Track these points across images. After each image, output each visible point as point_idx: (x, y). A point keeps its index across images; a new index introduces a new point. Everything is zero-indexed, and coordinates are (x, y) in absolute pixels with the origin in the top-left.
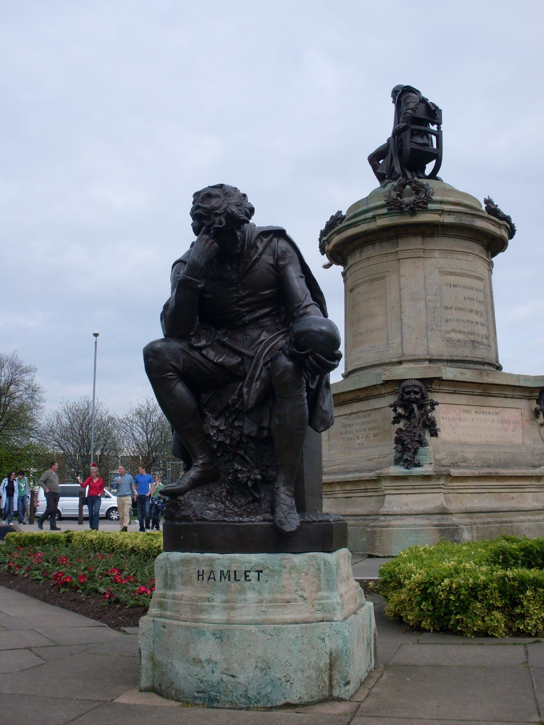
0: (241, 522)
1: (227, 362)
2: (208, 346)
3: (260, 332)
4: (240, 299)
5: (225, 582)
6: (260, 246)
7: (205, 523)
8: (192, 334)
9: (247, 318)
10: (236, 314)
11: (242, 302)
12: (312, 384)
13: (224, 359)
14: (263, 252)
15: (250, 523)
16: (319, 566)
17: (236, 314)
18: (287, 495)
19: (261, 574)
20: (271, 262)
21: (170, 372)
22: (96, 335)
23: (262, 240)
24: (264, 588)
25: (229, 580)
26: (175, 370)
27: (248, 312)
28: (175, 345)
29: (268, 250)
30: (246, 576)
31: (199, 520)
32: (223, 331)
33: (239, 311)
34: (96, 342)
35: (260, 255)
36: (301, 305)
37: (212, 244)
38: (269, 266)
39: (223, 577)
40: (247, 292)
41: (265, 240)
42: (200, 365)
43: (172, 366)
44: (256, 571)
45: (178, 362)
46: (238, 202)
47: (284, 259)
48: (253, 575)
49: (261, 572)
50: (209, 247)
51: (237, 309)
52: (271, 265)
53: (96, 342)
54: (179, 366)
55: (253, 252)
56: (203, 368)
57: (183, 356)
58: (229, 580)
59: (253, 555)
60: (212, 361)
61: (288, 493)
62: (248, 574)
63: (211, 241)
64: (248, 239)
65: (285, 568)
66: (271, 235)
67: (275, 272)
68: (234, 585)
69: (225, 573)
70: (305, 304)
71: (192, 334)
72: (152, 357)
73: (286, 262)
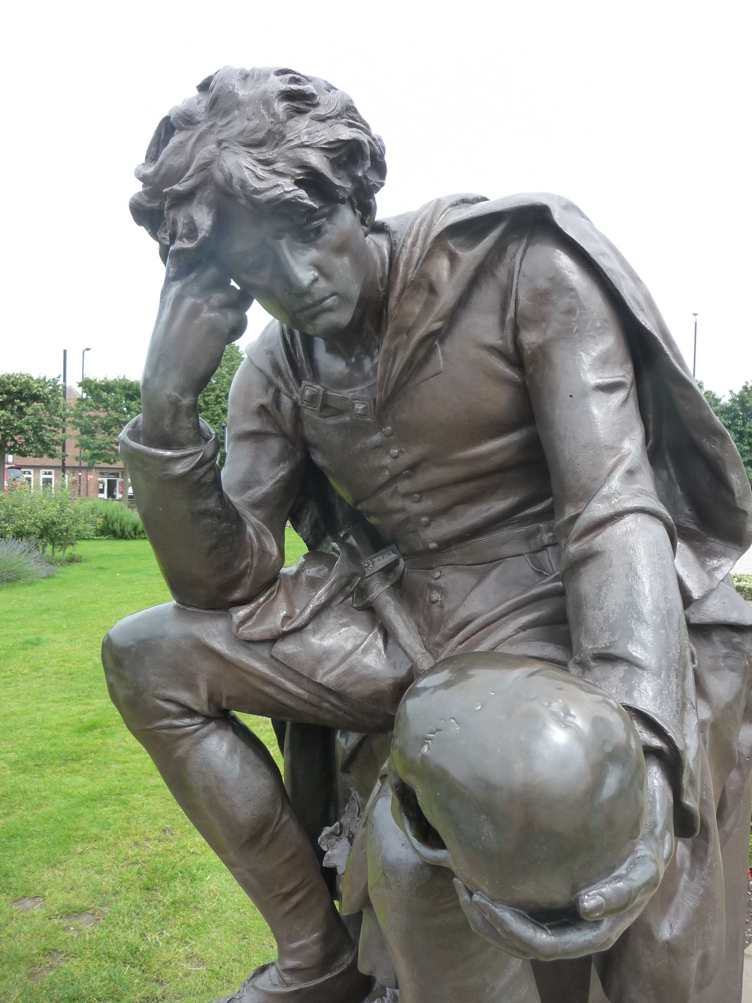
4: (395, 478)
8: (237, 595)
14: (463, 302)
17: (398, 517)
20: (493, 338)
22: (695, 315)
27: (434, 515)
29: (487, 296)
35: (452, 317)
36: (577, 517)
37: (195, 312)
41: (471, 256)
45: (190, 686)
46: (255, 131)
47: (539, 320)
51: (397, 503)
52: (493, 349)
55: (417, 309)
56: (281, 697)
63: (189, 302)
66: (495, 234)
70: (598, 509)
71: (237, 595)
73: (550, 333)
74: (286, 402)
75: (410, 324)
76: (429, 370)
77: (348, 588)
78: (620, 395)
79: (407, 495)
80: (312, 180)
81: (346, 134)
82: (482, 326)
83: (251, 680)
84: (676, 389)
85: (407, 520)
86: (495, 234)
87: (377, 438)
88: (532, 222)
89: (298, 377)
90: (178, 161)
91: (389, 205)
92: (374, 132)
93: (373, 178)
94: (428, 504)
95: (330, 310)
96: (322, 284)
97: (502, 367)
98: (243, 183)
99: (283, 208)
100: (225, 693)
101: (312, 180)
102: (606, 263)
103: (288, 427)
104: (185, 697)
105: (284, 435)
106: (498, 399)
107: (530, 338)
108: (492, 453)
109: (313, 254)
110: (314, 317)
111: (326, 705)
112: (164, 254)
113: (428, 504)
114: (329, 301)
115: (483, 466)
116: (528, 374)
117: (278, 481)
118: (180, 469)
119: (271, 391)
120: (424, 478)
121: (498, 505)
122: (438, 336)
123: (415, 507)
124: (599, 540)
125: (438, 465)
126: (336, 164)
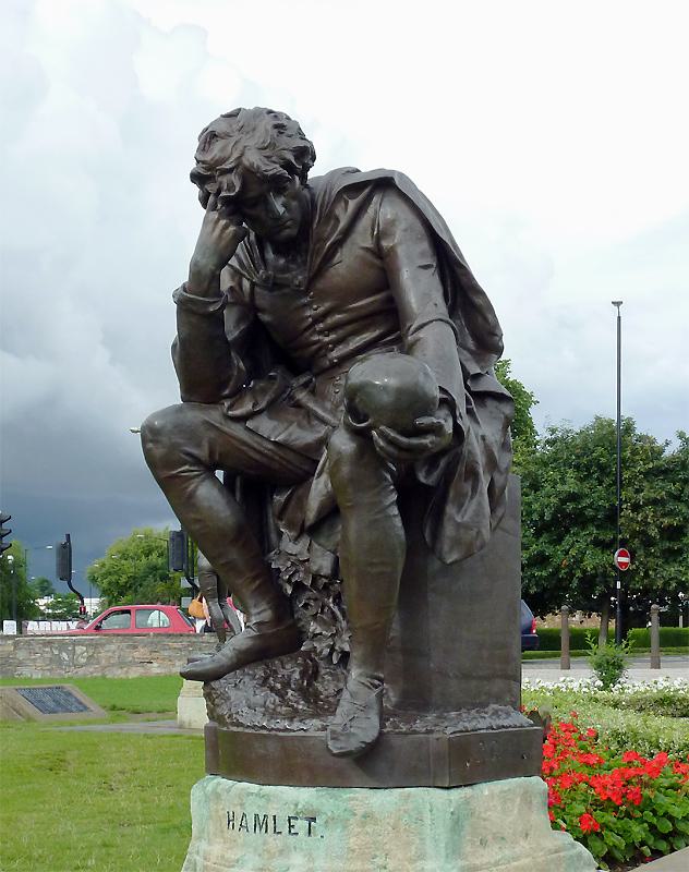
0: (286, 730)
1: (296, 439)
2: (260, 412)
3: (349, 382)
4: (317, 320)
5: (260, 836)
6: (344, 215)
7: (240, 729)
8: (227, 392)
9: (335, 354)
10: (315, 347)
11: (321, 325)
12: (429, 473)
13: (290, 435)
15: (302, 733)
16: (420, 813)
17: (315, 347)
21: (185, 464)
22: (618, 304)
24: (318, 848)
26: (196, 461)
27: (337, 343)
28: (196, 416)
31: (233, 724)
32: (303, 380)
34: (619, 317)
37: (226, 227)
39: (258, 826)
40: (327, 305)
41: (352, 204)
42: (244, 448)
43: (188, 454)
44: (307, 819)
45: (199, 445)
48: (301, 825)
49: (314, 819)
50: (220, 236)
51: (316, 338)
52: (367, 249)
53: (619, 317)
54: (203, 453)
56: (252, 454)
59: (303, 789)
60: (268, 439)
63: (223, 222)
64: (322, 206)
66: (367, 191)
68: (274, 842)
69: (261, 818)
71: (227, 392)
72: (151, 441)
74: (246, 284)
78: (433, 270)
79: (321, 332)
80: (287, 165)
83: (234, 442)
84: (459, 271)
85: (320, 349)
87: (306, 300)
88: (385, 184)
91: (311, 174)
94: (333, 336)
95: (289, 227)
96: (287, 214)
98: (258, 167)
99: (276, 179)
100: (218, 450)
101: (287, 165)
102: (420, 206)
103: (247, 299)
104: (195, 451)
106: (371, 275)
107: (385, 244)
109: (282, 199)
110: (280, 231)
111: (277, 458)
112: (204, 201)
113: (333, 336)
114: (289, 223)
119: (237, 278)
120: (330, 321)
121: (368, 336)
122: (339, 244)
123: (327, 339)
124: (421, 334)
126: (296, 158)
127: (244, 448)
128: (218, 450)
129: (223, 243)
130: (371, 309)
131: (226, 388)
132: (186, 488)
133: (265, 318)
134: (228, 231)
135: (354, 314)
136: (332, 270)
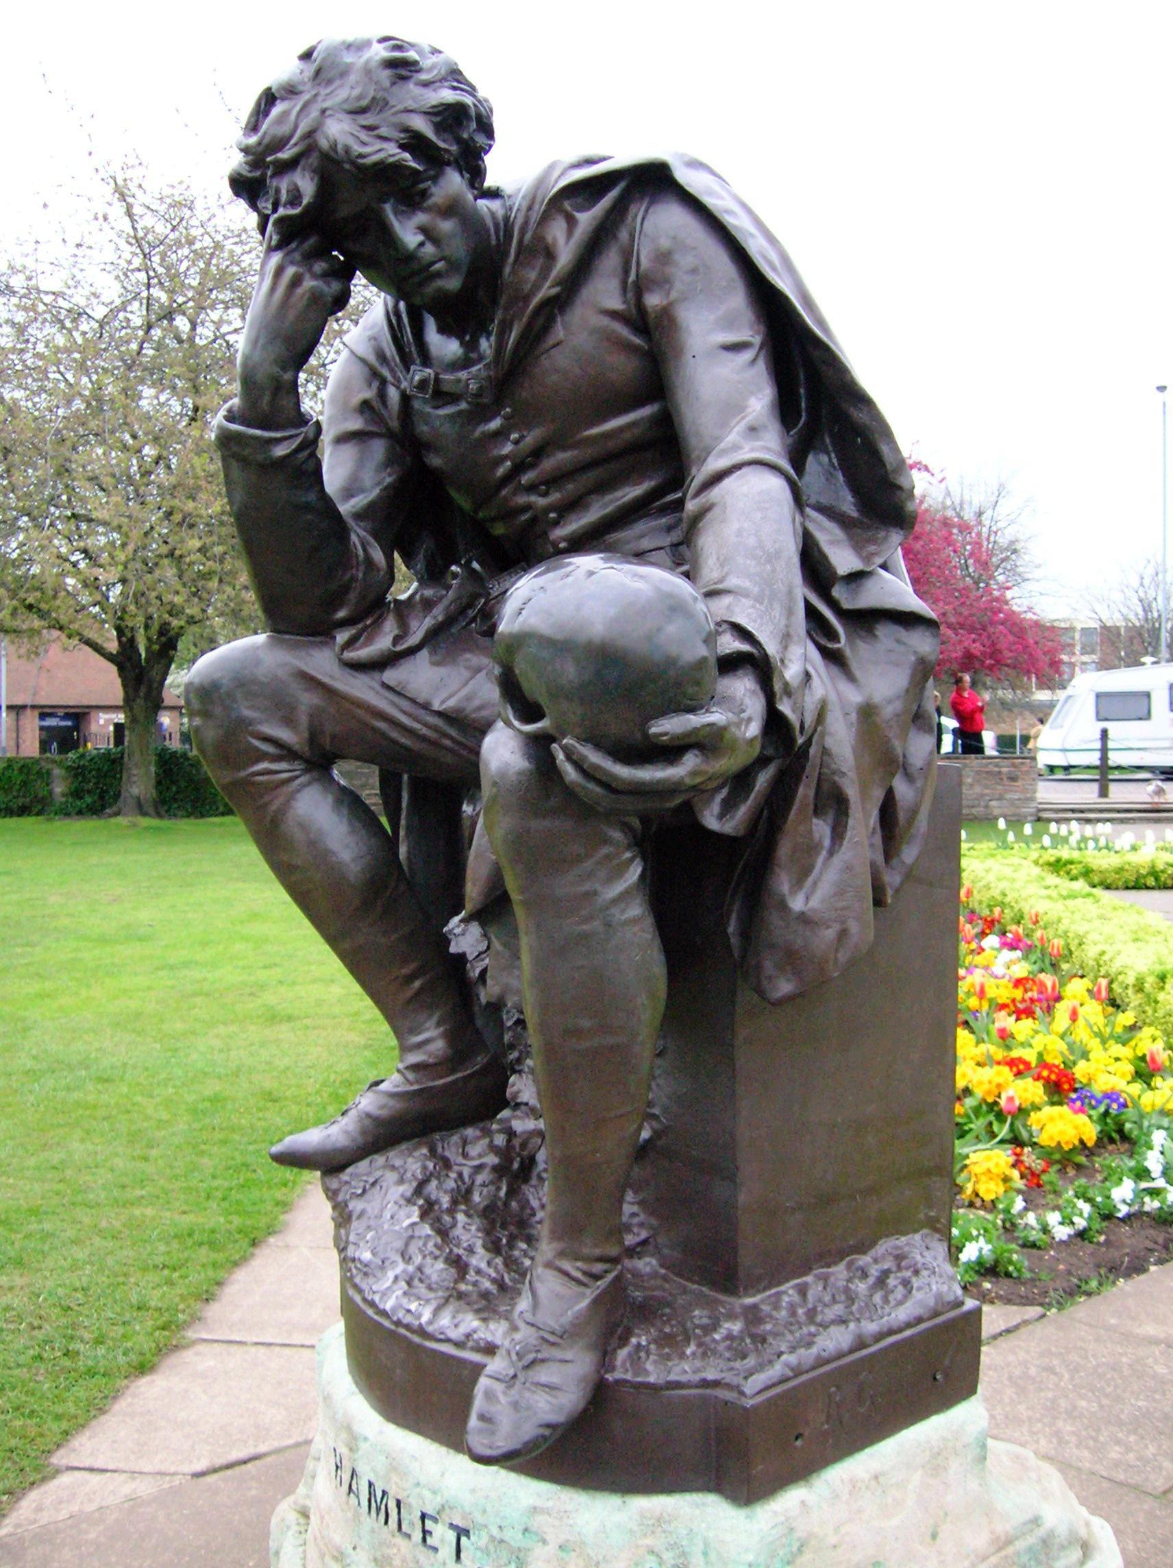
4: (520, 467)
8: (341, 614)
10: (525, 517)
12: (728, 806)
17: (525, 517)
18: (567, 1274)
19: (464, 1539)
20: (616, 304)
22: (1162, 389)
23: (571, 222)
25: (386, 1522)
26: (286, 752)
29: (610, 261)
30: (425, 1533)
33: (528, 507)
37: (296, 282)
38: (606, 321)
41: (587, 219)
42: (382, 725)
44: (452, 1526)
45: (289, 721)
46: (359, 98)
48: (442, 1535)
49: (467, 1533)
51: (522, 500)
52: (614, 314)
56: (394, 734)
57: (307, 700)
58: (386, 1522)
60: (426, 706)
61: (567, 1265)
62: (429, 1524)
63: (291, 271)
65: (544, 1542)
66: (613, 194)
67: (637, 341)
70: (715, 464)
71: (341, 614)
74: (393, 394)
75: (526, 291)
76: (551, 341)
77: (470, 612)
78: (748, 355)
79: (532, 488)
80: (415, 143)
81: (448, 95)
82: (605, 291)
83: (359, 712)
84: (816, 354)
85: (534, 520)
86: (613, 194)
87: (495, 424)
88: (652, 180)
89: (406, 362)
90: (285, 129)
92: (481, 93)
93: (481, 140)
94: (555, 497)
95: (438, 275)
96: (429, 249)
97: (624, 332)
98: (347, 150)
99: (385, 173)
100: (329, 728)
102: (737, 222)
103: (395, 424)
104: (284, 734)
105: (390, 435)
106: (623, 368)
107: (653, 300)
108: (621, 430)
109: (421, 218)
110: (421, 284)
111: (447, 742)
113: (555, 497)
114: (438, 266)
115: (611, 445)
116: (651, 339)
117: (386, 488)
118: (280, 451)
119: (376, 384)
120: (549, 464)
121: (632, 492)
122: (559, 304)
123: (541, 502)
124: (716, 493)
125: (564, 448)
126: (439, 128)
127: (382, 725)
128: (329, 728)
129: (291, 315)
130: (627, 436)
131: (340, 606)
132: (266, 804)
133: (435, 461)
134: (299, 291)
135: (588, 453)
136: (545, 362)
